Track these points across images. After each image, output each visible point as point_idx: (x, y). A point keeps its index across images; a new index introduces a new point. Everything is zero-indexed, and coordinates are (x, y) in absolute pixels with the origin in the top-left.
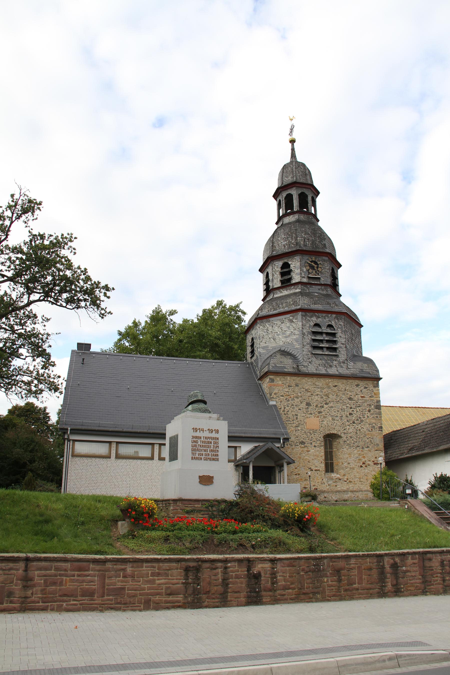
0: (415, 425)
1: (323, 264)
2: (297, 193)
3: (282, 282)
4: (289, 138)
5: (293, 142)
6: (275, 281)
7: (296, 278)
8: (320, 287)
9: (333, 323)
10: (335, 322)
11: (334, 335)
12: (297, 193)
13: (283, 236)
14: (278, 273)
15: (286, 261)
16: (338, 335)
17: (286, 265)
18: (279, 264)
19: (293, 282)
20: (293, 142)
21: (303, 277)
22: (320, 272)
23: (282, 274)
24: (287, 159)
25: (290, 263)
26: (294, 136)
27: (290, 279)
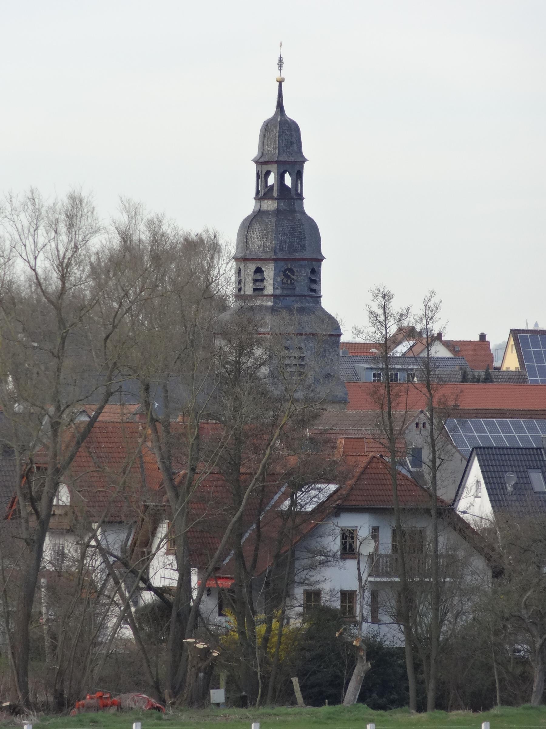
0: (500, 410)
1: (300, 270)
2: (282, 148)
3: (255, 290)
4: (277, 74)
5: (280, 82)
6: (247, 286)
7: (269, 290)
8: (293, 298)
9: (303, 345)
10: (305, 344)
11: (303, 358)
12: (282, 148)
13: (258, 234)
14: (250, 278)
15: (259, 265)
16: (306, 359)
17: (259, 271)
18: (252, 267)
19: (266, 292)
20: (280, 82)
21: (276, 289)
22: (296, 281)
23: (255, 281)
24: (270, 112)
25: (263, 269)
26: (284, 74)
27: (262, 289)
